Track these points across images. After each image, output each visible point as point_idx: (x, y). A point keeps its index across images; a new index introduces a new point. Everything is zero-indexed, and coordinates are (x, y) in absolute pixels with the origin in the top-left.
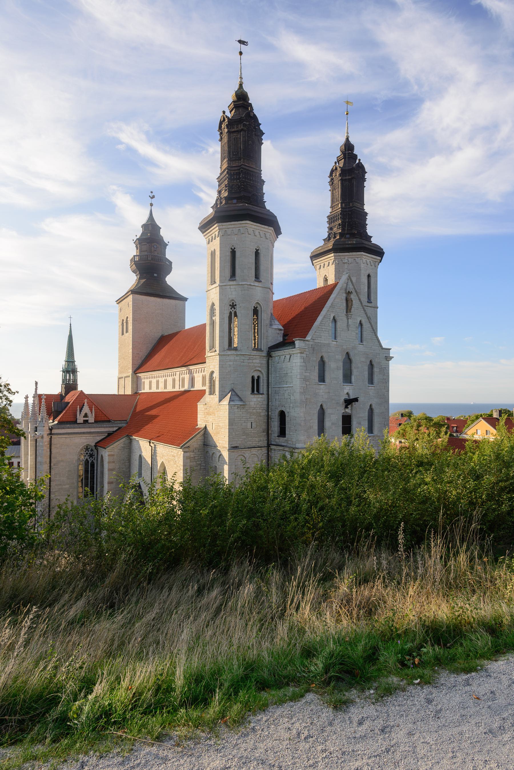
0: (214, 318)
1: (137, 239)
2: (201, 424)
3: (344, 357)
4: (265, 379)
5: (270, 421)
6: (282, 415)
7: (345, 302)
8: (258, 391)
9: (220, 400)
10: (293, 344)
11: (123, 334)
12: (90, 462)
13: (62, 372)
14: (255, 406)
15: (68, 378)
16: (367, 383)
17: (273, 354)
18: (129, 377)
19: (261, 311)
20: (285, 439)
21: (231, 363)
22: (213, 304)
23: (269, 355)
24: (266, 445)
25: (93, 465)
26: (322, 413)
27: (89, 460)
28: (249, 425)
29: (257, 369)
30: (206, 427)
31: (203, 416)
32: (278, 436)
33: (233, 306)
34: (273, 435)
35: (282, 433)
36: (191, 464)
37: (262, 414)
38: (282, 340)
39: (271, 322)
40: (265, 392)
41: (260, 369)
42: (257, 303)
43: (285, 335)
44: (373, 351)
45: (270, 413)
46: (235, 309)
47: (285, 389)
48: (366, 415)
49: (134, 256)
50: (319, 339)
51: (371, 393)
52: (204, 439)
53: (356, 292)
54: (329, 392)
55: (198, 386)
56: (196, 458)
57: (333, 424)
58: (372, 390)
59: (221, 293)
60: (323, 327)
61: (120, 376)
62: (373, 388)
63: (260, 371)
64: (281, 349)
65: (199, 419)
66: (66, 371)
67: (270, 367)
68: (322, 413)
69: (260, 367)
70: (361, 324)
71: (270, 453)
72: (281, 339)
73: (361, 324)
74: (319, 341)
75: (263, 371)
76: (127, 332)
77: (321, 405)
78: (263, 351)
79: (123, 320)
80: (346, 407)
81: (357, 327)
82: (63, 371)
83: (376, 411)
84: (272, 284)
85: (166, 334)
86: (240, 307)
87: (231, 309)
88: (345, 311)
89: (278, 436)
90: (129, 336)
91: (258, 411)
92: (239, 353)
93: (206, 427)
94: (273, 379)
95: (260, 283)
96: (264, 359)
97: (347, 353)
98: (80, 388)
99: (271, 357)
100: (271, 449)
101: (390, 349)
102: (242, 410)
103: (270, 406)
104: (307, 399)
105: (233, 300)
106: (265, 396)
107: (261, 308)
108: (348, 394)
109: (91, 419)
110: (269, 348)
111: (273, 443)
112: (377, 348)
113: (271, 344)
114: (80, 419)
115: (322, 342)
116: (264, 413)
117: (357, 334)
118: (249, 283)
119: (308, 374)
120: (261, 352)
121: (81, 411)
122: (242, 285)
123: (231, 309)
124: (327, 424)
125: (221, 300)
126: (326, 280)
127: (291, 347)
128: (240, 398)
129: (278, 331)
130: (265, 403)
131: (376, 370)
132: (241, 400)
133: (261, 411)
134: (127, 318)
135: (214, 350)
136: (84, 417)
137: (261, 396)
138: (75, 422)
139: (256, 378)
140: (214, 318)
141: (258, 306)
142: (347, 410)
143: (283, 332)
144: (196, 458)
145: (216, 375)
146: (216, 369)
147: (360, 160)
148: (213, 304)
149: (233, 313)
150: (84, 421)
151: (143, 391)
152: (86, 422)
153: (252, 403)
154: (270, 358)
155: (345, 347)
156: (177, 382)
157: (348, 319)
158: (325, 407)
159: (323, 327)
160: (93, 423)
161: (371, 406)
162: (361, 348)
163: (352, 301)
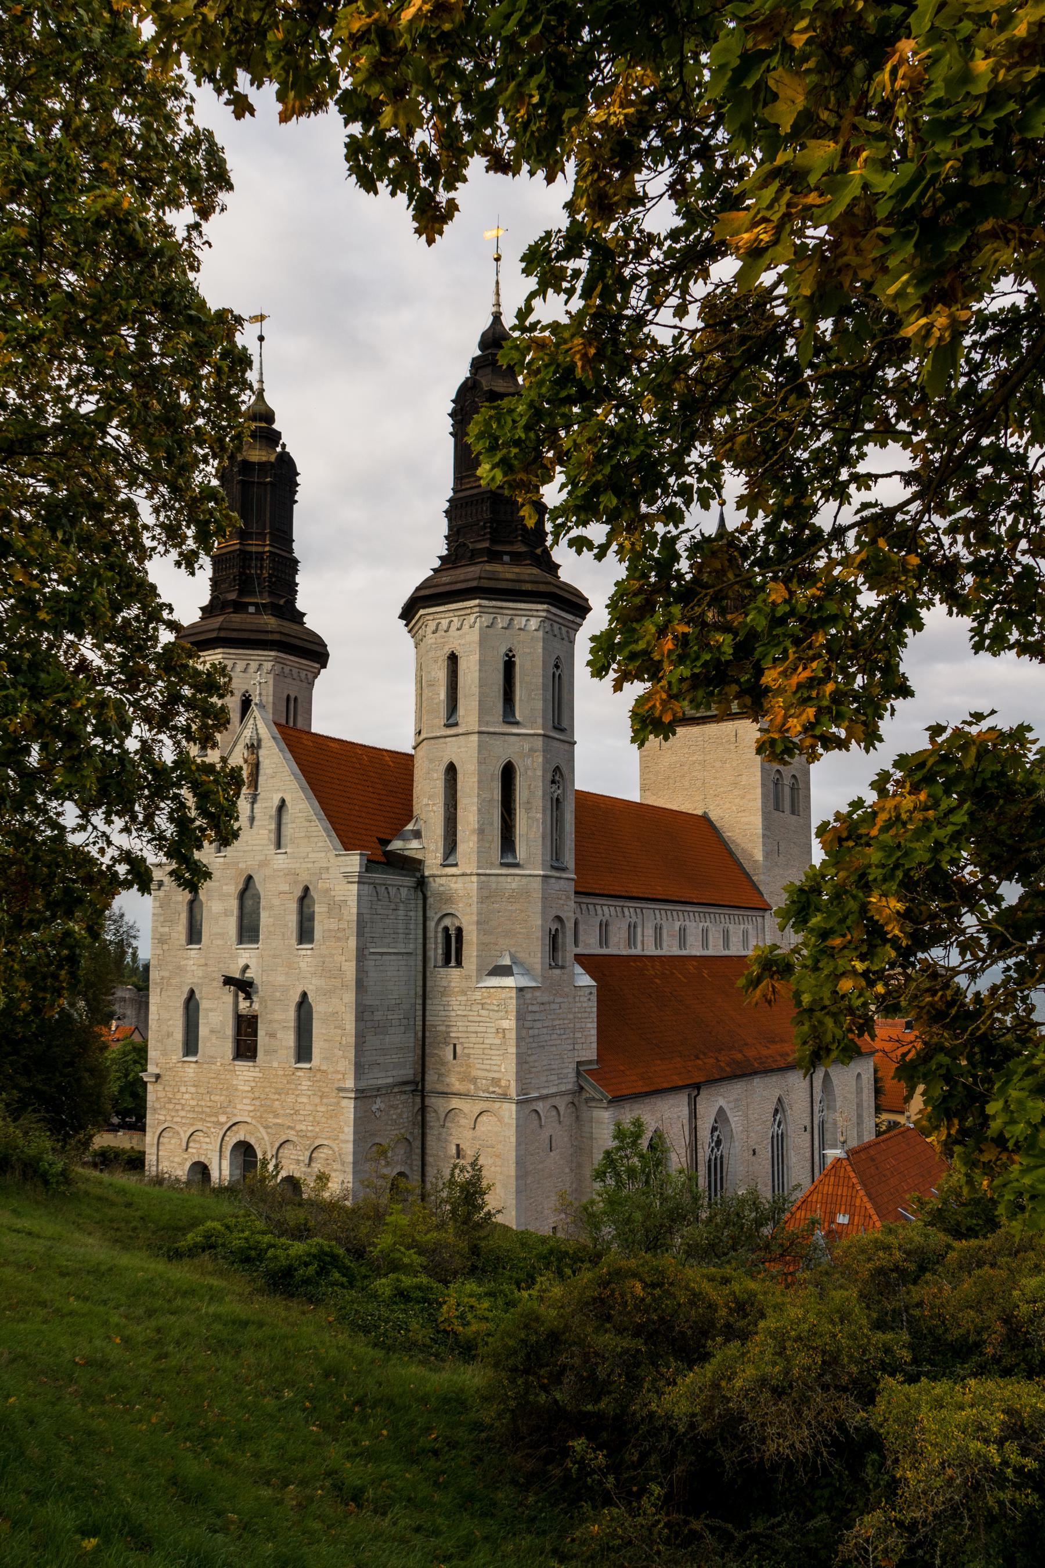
44: (310, 865)
48: (292, 1014)
51: (303, 965)
54: (206, 965)
57: (212, 1031)
58: (306, 957)
62: (309, 952)
77: (192, 992)
81: (271, 817)
83: (319, 1009)
104: (162, 978)
112: (323, 855)
117: (270, 831)
155: (242, 866)
161: (304, 995)
162: (280, 861)
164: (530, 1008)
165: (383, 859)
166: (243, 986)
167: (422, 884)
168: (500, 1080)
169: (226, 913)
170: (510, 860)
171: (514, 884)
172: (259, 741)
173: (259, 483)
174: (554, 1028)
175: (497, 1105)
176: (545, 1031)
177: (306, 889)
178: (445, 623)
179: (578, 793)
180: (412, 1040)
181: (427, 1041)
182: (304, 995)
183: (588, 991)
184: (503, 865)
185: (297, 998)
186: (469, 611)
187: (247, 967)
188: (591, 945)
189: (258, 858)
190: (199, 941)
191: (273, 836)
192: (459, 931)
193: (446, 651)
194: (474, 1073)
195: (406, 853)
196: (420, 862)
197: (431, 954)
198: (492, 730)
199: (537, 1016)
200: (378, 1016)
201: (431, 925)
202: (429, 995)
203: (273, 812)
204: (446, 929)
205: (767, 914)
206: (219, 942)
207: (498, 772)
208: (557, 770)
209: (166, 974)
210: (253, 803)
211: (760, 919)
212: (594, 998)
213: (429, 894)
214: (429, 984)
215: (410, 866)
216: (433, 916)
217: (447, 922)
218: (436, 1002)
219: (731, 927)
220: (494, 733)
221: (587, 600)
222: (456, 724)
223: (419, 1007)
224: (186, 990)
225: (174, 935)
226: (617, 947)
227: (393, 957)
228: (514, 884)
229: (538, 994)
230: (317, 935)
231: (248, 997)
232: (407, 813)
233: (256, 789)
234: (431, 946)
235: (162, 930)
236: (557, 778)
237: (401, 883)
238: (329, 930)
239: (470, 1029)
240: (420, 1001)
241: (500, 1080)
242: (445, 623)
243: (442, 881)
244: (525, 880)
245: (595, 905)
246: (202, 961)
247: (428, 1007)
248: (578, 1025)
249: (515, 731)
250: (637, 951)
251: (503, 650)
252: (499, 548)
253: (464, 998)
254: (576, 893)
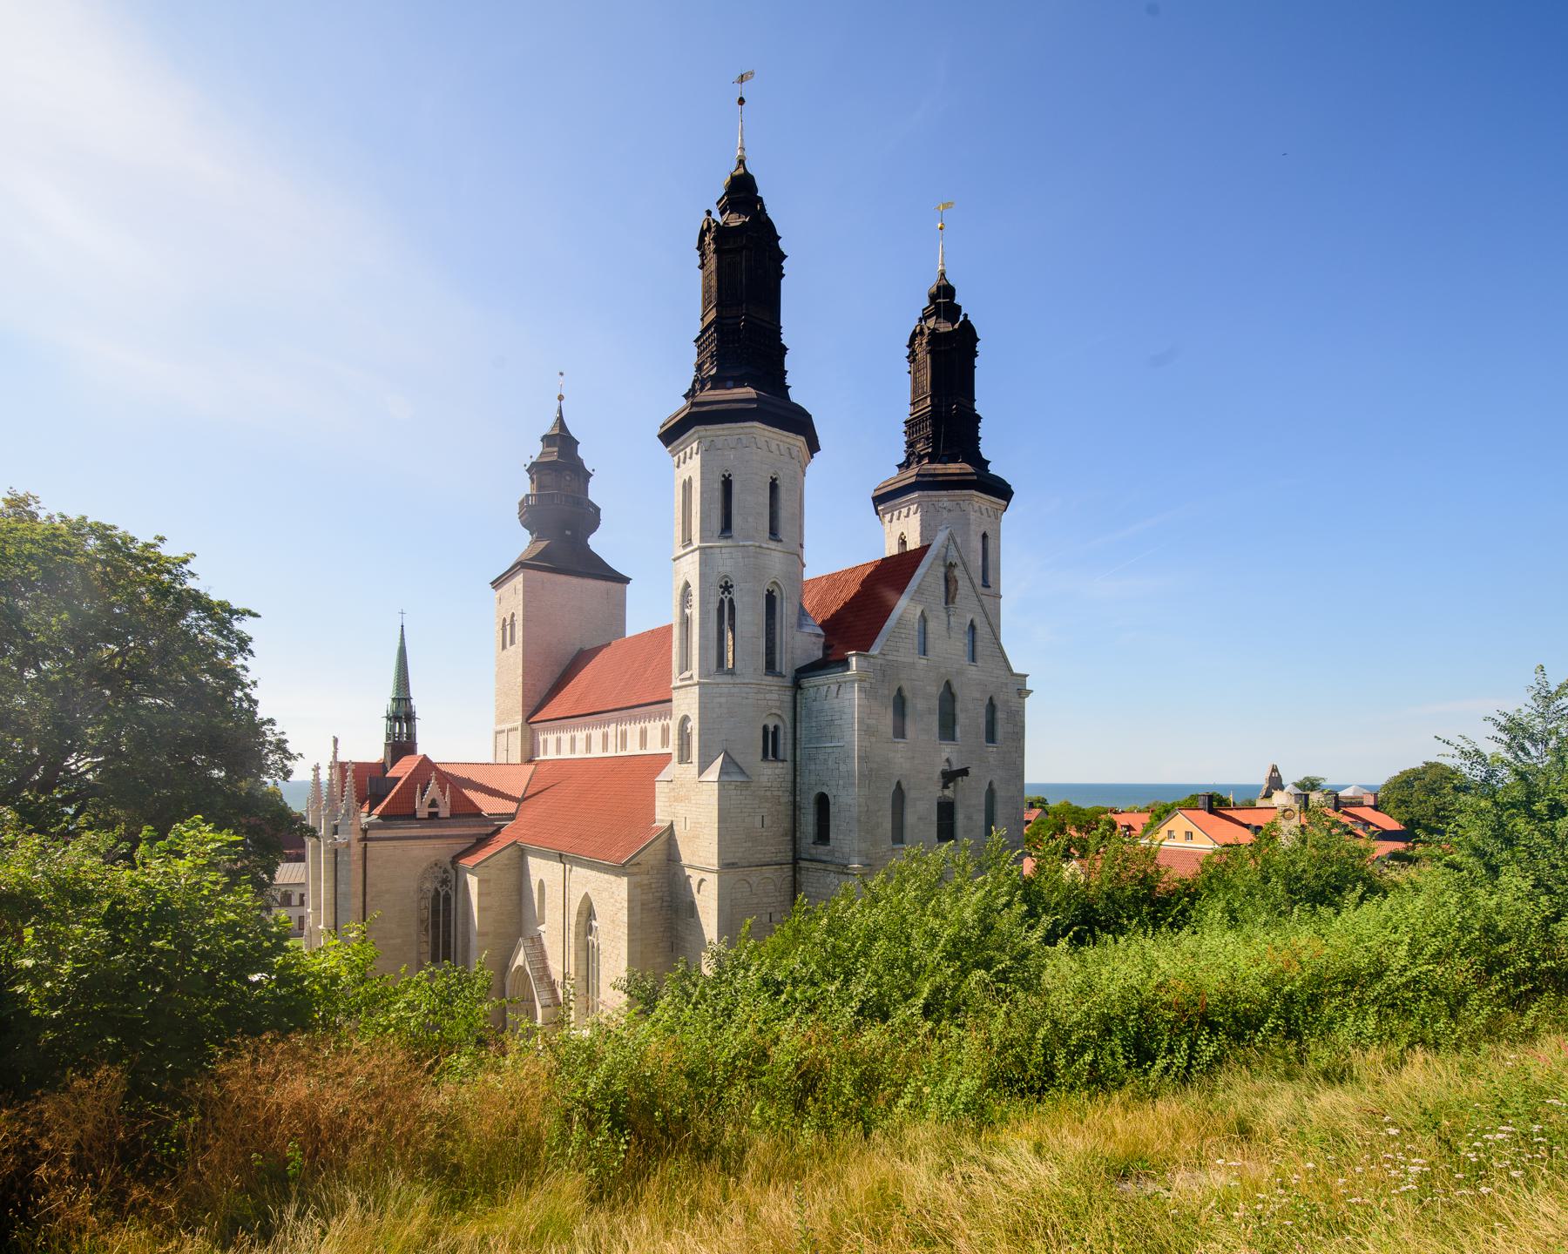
0: (688, 611)
2: (662, 817)
3: (942, 689)
4: (789, 730)
5: (798, 813)
6: (823, 802)
7: (942, 582)
8: (775, 754)
9: (701, 773)
10: (845, 663)
11: (504, 647)
12: (442, 894)
13: (385, 720)
14: (769, 784)
15: (397, 731)
16: (984, 740)
17: (806, 683)
18: (516, 729)
19: (782, 599)
20: (828, 847)
21: (723, 700)
22: (687, 585)
23: (797, 686)
24: (790, 859)
25: (447, 899)
26: (899, 796)
27: (440, 889)
28: (758, 823)
29: (774, 711)
30: (672, 825)
31: (667, 804)
32: (814, 843)
33: (727, 588)
34: (804, 841)
35: (823, 835)
36: (644, 897)
37: (783, 800)
38: (821, 656)
39: (799, 619)
40: (789, 757)
41: (779, 712)
42: (774, 583)
43: (827, 647)
44: (994, 680)
45: (798, 798)
46: (729, 593)
47: (830, 750)
50: (895, 653)
51: (991, 759)
52: (669, 849)
53: (964, 564)
54: (913, 758)
55: (654, 747)
56: (653, 886)
57: (919, 819)
59: (704, 563)
60: (902, 631)
61: (499, 728)
63: (779, 716)
64: (821, 672)
65: (657, 810)
66: (394, 718)
67: (798, 709)
68: (899, 796)
69: (779, 708)
70: (972, 627)
71: (798, 876)
72: (819, 654)
73: (972, 627)
74: (895, 658)
75: (784, 716)
76: (512, 643)
78: (784, 676)
79: (505, 620)
80: (945, 786)
81: (965, 632)
82: (388, 718)
83: (1001, 793)
84: (802, 546)
85: (588, 647)
86: (741, 590)
87: (723, 593)
88: (943, 600)
89: (814, 843)
90: (516, 652)
91: (775, 793)
92: (738, 681)
93: (672, 825)
94: (804, 732)
95: (779, 544)
96: (788, 693)
97: (948, 684)
98: (421, 751)
99: (801, 689)
100: (800, 868)
101: (1026, 676)
102: (744, 793)
103: (798, 785)
104: (871, 770)
105: (726, 576)
106: (789, 765)
107: (782, 594)
108: (948, 760)
109: (444, 812)
110: (796, 670)
111: (803, 856)
113: (800, 663)
114: (422, 811)
115: (899, 659)
116: (786, 798)
117: (965, 645)
118: (757, 544)
119: (874, 722)
120: (780, 679)
121: (423, 795)
122: (744, 546)
123: (723, 593)
124: (910, 818)
125: (703, 576)
126: (903, 543)
127: (840, 669)
128: (741, 769)
129: (814, 639)
130: (789, 778)
131: (1000, 715)
132: (742, 772)
133: (780, 793)
134: (513, 615)
135: (687, 674)
136: (430, 806)
137: (780, 765)
138: (412, 816)
139: (771, 729)
140: (688, 611)
141: (776, 589)
142: (947, 792)
143: (823, 640)
144: (653, 886)
145: (694, 725)
146: (693, 711)
148: (687, 585)
149: (726, 601)
150: (430, 813)
151: (542, 757)
152: (433, 816)
153: (764, 779)
154: (799, 691)
155: (943, 670)
156: (611, 740)
157: (949, 616)
158: (904, 786)
159: (902, 631)
160: (447, 818)
161: (991, 784)
162: (972, 672)
163: (956, 581)
190: (903, 736)
235: (869, 721)
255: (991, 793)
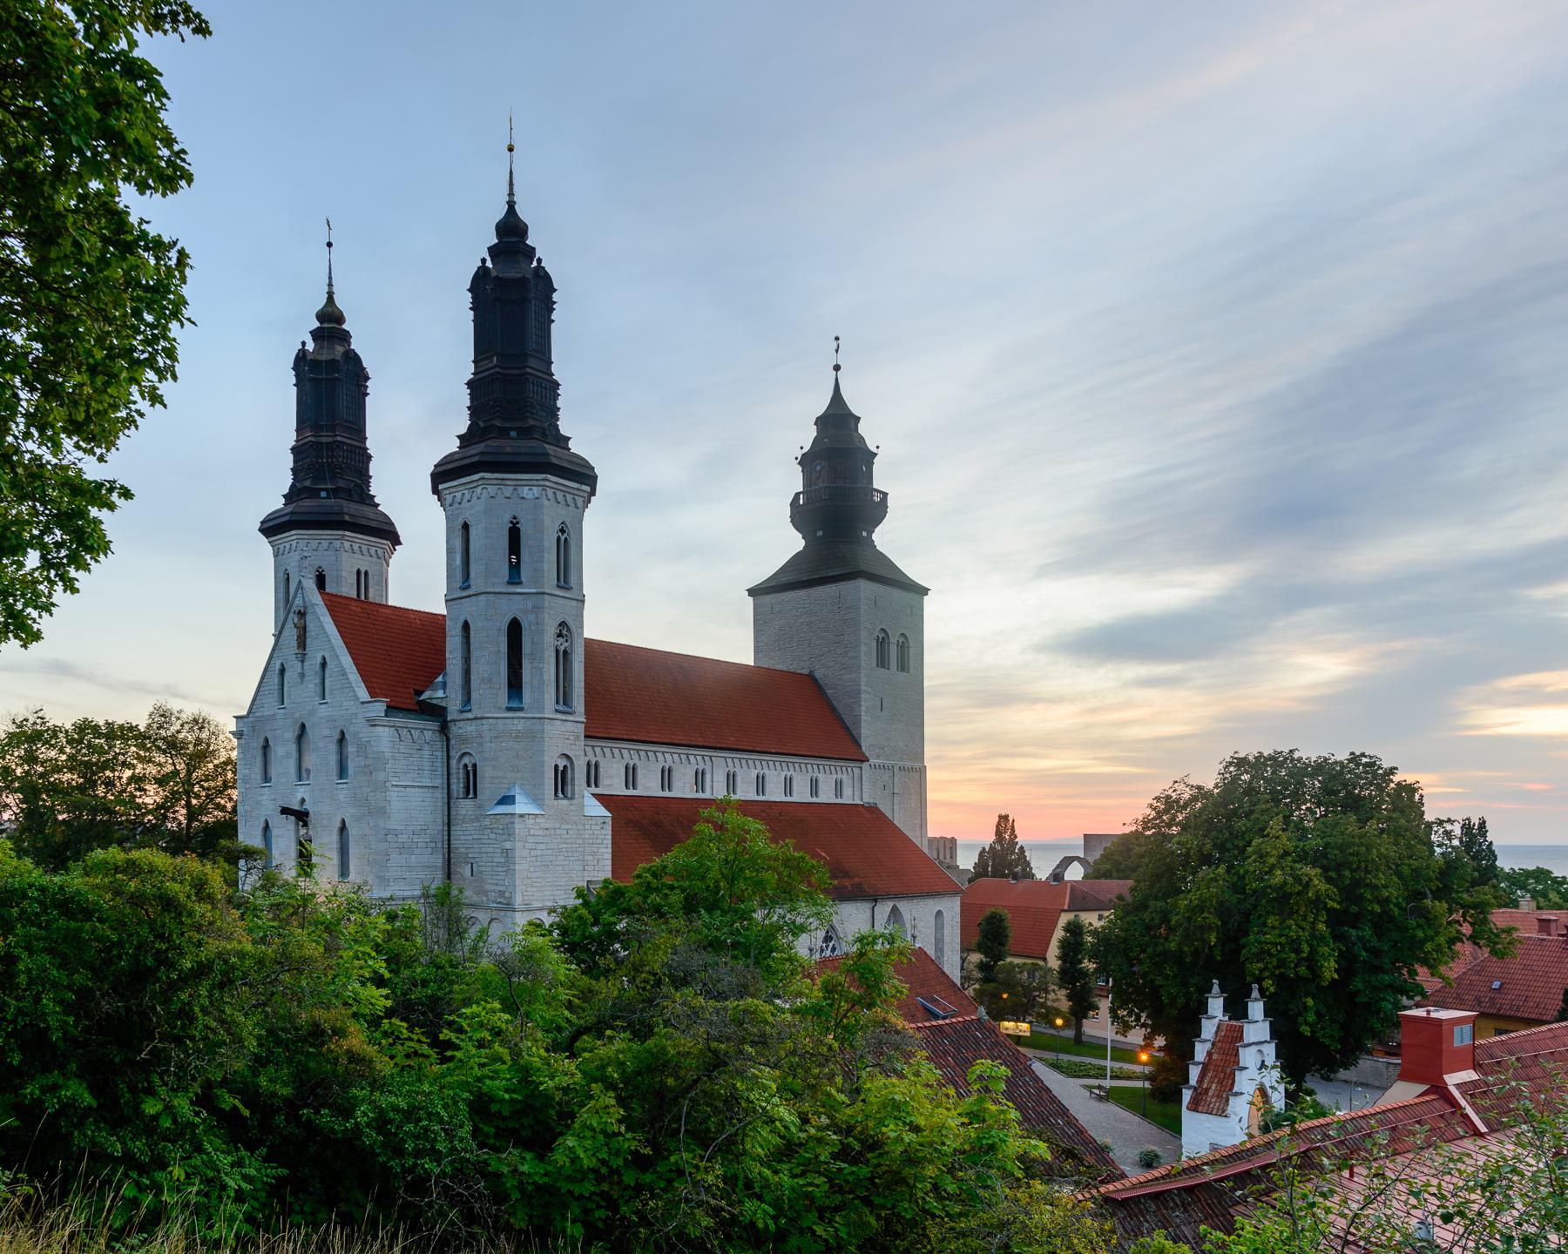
1: (803, 455)
48: (335, 837)
49: (797, 495)
51: (341, 796)
58: (343, 792)
112: (353, 703)
117: (316, 685)
131: (351, 749)
147: (539, 261)
155: (297, 715)
161: (343, 822)
162: (323, 711)
164: (532, 832)
165: (417, 708)
166: (302, 817)
167: (444, 729)
168: (504, 892)
169: (287, 756)
170: (514, 705)
171: (520, 726)
172: (306, 608)
173: (327, 380)
174: (560, 850)
175: (503, 913)
176: (550, 852)
177: (343, 733)
178: (458, 495)
179: (589, 643)
180: (440, 860)
181: (452, 861)
182: (343, 822)
183: (601, 820)
184: (509, 709)
185: (338, 825)
186: (475, 484)
187: (303, 801)
188: (614, 784)
189: (308, 708)
191: (318, 689)
192: (475, 766)
193: (460, 521)
194: (488, 887)
195: (434, 702)
196: (444, 709)
197: (454, 787)
198: (497, 590)
199: (540, 839)
200: (403, 838)
201: (453, 762)
202: (453, 822)
203: (318, 667)
204: (466, 766)
205: (865, 765)
206: (284, 780)
207: (505, 627)
208: (563, 624)
209: (248, 808)
210: (303, 661)
211: (856, 771)
212: (609, 828)
213: (451, 736)
214: (453, 813)
215: (435, 712)
216: (455, 754)
217: (466, 760)
218: (458, 828)
219: (821, 777)
220: (500, 593)
221: (593, 468)
222: (469, 587)
223: (446, 833)
224: (263, 820)
225: (253, 776)
226: (649, 786)
227: (417, 790)
228: (520, 726)
229: (539, 820)
230: (351, 772)
231: (305, 825)
232: (441, 667)
233: (305, 649)
234: (454, 780)
236: (564, 632)
237: (426, 730)
238: (359, 767)
239: (484, 850)
240: (446, 828)
241: (504, 892)
242: (458, 495)
243: (461, 724)
244: (529, 722)
245: (655, 752)
246: (273, 797)
247: (452, 833)
248: (588, 850)
249: (519, 590)
250: (707, 795)
251: (507, 518)
252: (508, 425)
253: (478, 824)
254: (586, 737)
255: (343, 828)
